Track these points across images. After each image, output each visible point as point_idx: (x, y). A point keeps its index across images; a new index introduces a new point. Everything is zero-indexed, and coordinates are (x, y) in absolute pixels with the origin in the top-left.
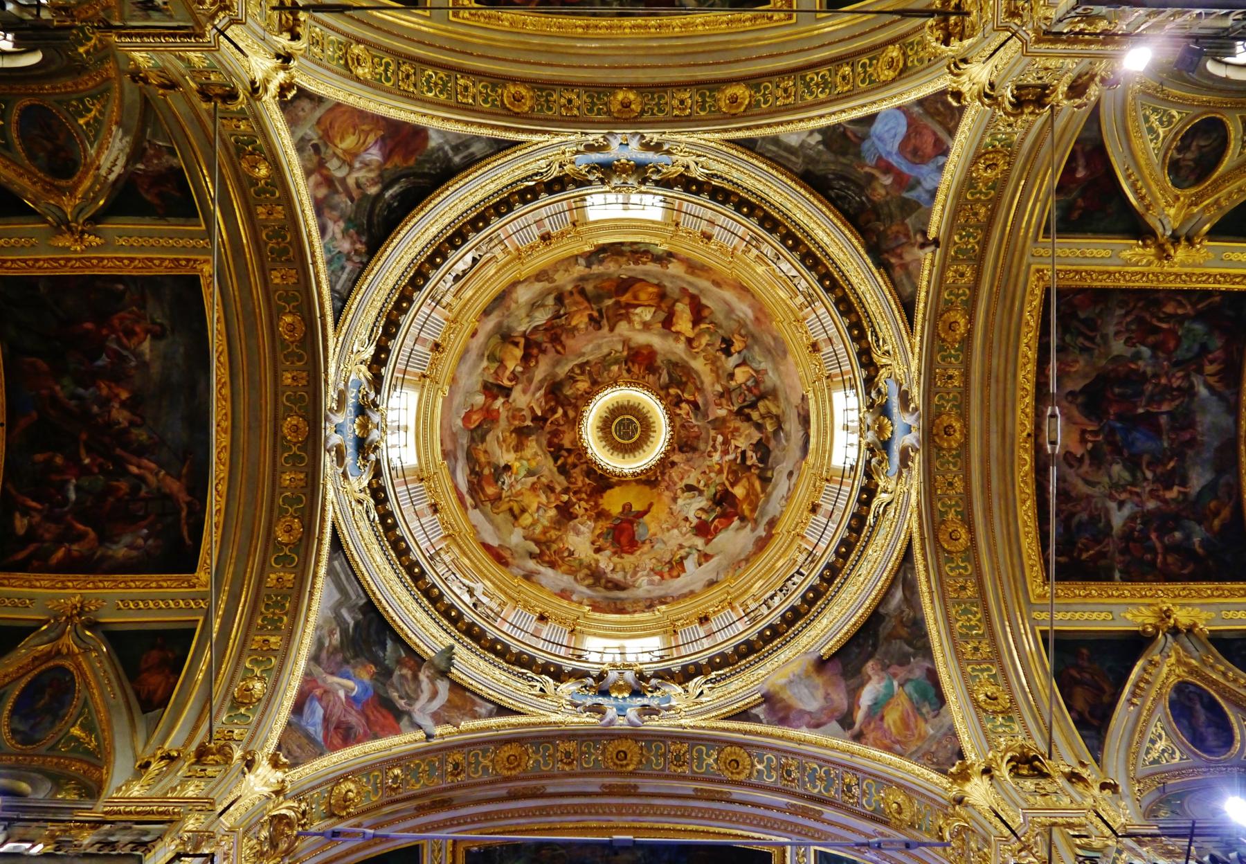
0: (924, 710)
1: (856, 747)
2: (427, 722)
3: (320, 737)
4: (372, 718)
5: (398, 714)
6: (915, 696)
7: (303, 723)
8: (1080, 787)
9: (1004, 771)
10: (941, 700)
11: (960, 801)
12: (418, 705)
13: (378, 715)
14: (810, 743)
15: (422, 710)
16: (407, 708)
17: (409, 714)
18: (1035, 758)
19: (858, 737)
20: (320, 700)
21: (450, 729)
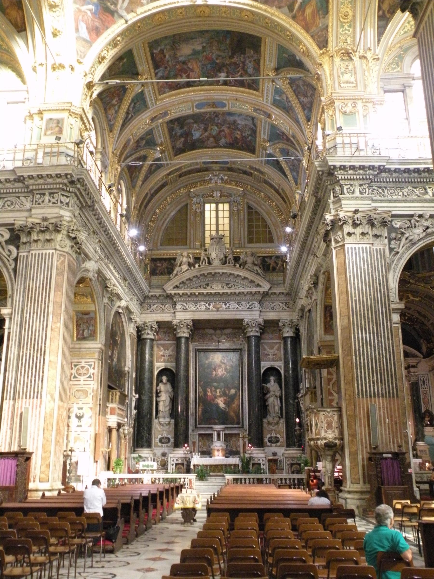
0: (320, 12)
1: (292, 22)
2: (124, 13)
3: (88, 39)
4: (103, 19)
5: (112, 13)
6: (319, 4)
7: (81, 35)
8: (365, 61)
9: (337, 60)
10: (327, 12)
11: (321, 64)
12: (119, 6)
13: (105, 16)
14: (276, 16)
15: (121, 8)
16: (115, 9)
17: (117, 12)
18: (351, 53)
19: (294, 18)
20: (83, 21)
21: (134, 15)
